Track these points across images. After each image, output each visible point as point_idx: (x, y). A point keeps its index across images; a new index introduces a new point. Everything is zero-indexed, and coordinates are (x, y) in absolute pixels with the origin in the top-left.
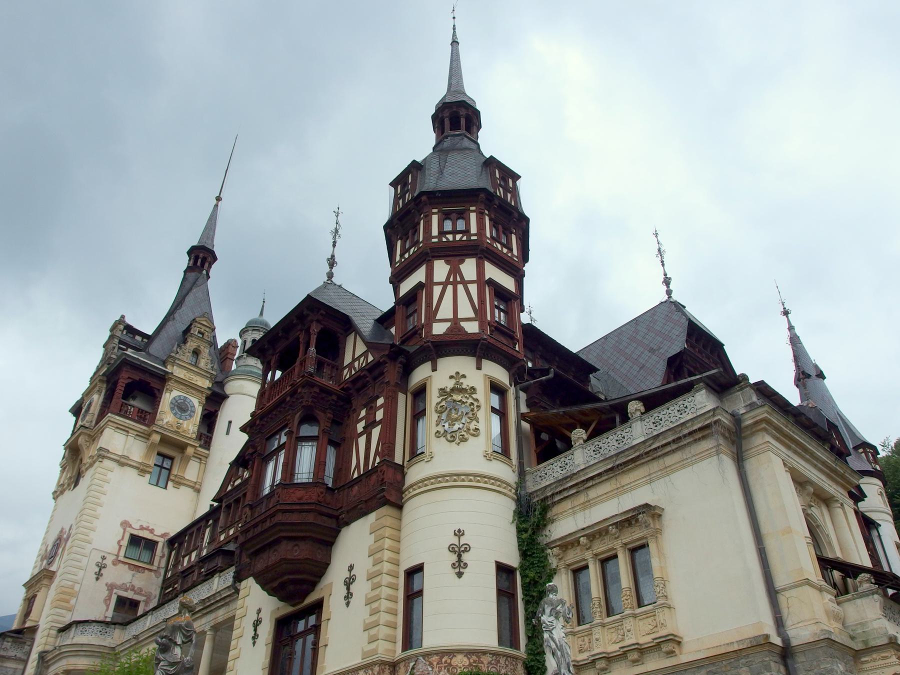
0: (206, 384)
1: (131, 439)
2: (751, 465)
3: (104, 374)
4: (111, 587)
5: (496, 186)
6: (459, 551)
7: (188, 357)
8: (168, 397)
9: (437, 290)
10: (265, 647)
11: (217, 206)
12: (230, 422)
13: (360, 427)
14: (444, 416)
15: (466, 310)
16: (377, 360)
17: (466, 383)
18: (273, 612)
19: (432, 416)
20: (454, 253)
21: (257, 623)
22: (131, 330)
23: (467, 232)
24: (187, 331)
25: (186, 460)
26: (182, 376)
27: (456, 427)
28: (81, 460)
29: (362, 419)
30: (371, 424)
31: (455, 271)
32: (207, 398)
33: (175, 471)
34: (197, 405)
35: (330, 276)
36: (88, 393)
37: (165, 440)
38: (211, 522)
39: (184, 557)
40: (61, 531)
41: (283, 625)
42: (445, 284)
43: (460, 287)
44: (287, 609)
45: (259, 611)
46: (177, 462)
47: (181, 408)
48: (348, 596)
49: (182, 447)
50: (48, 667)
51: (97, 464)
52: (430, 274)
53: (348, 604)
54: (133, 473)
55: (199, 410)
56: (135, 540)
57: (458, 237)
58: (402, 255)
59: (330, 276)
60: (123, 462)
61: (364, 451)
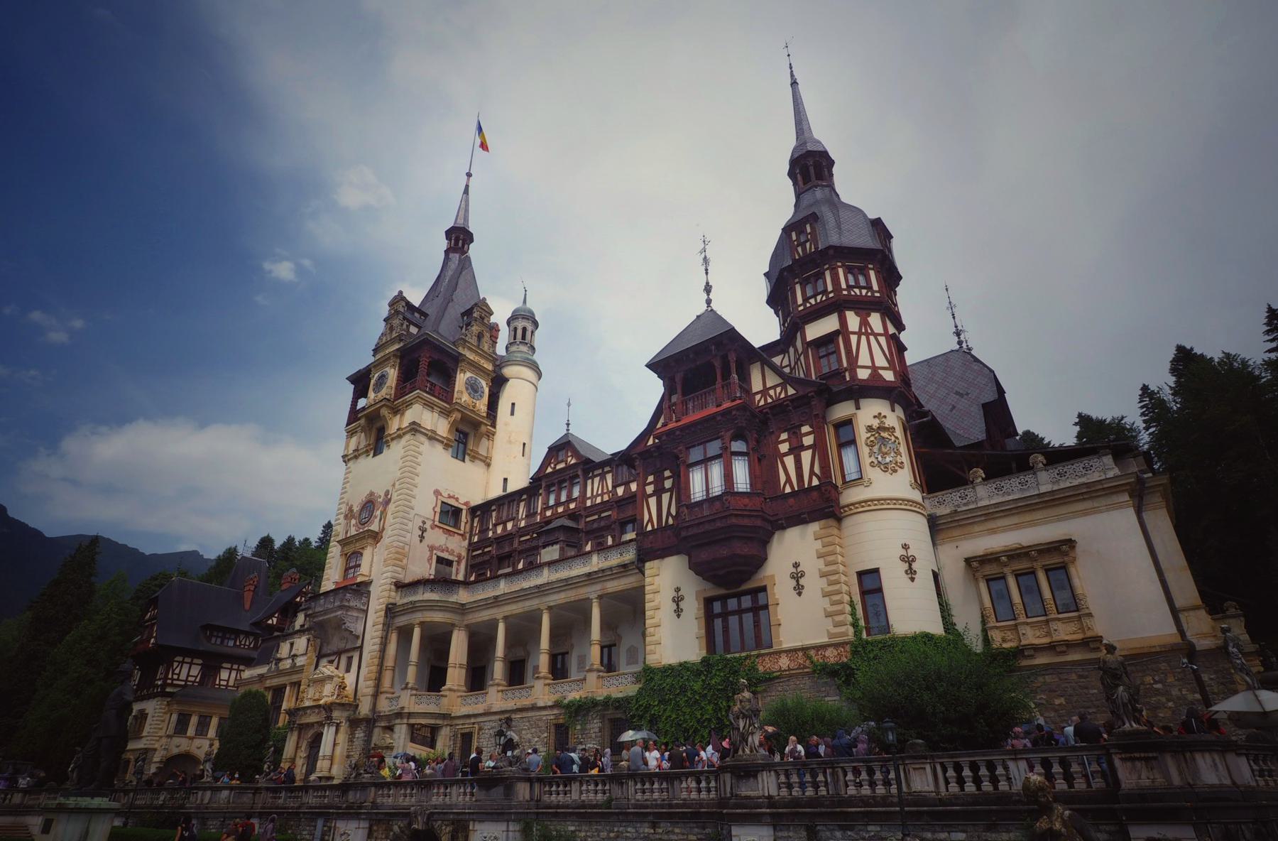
1: (436, 415)
2: (1145, 515)
4: (432, 548)
6: (909, 560)
7: (474, 341)
8: (462, 378)
9: (854, 339)
10: (695, 622)
11: (467, 186)
12: (513, 404)
13: (784, 448)
14: (876, 449)
15: (881, 361)
16: (801, 393)
18: (698, 593)
19: (865, 451)
20: (864, 307)
21: (678, 600)
22: (409, 306)
23: (869, 288)
24: (468, 313)
25: (479, 438)
27: (888, 459)
28: (382, 430)
29: (784, 441)
30: (796, 450)
31: (865, 323)
32: (492, 380)
33: (470, 446)
34: (485, 386)
35: (709, 302)
36: (378, 364)
37: (465, 419)
39: (495, 525)
40: (372, 494)
41: (708, 602)
42: (859, 334)
43: (872, 338)
44: (714, 591)
45: (678, 590)
47: (473, 388)
48: (799, 589)
49: (476, 425)
50: (393, 618)
51: (408, 437)
52: (843, 322)
53: (800, 594)
54: (439, 448)
55: (487, 390)
57: (864, 292)
58: (806, 300)
59: (709, 302)
60: (432, 437)
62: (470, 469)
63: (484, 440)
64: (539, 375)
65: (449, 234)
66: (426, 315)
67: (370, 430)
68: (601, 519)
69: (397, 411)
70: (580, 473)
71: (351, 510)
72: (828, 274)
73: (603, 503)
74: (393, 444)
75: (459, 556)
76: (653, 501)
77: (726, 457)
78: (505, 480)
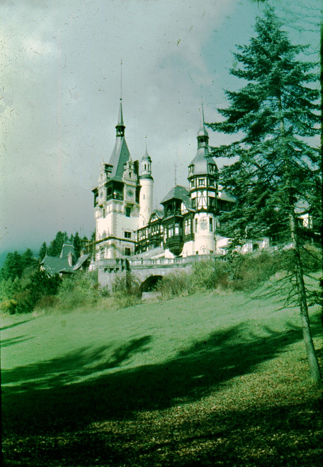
0: (134, 184)
3: (106, 184)
5: (210, 171)
9: (199, 199)
12: (144, 195)
13: (186, 224)
15: (204, 204)
17: (205, 219)
20: (202, 189)
23: (204, 185)
31: (202, 194)
34: (134, 190)
35: (176, 183)
37: (128, 204)
38: (147, 229)
40: (104, 231)
42: (200, 197)
46: (131, 209)
47: (130, 193)
49: (132, 205)
56: (126, 233)
59: (176, 183)
61: (187, 230)
64: (153, 182)
66: (112, 166)
67: (101, 210)
72: (195, 181)
74: (108, 215)
77: (174, 228)
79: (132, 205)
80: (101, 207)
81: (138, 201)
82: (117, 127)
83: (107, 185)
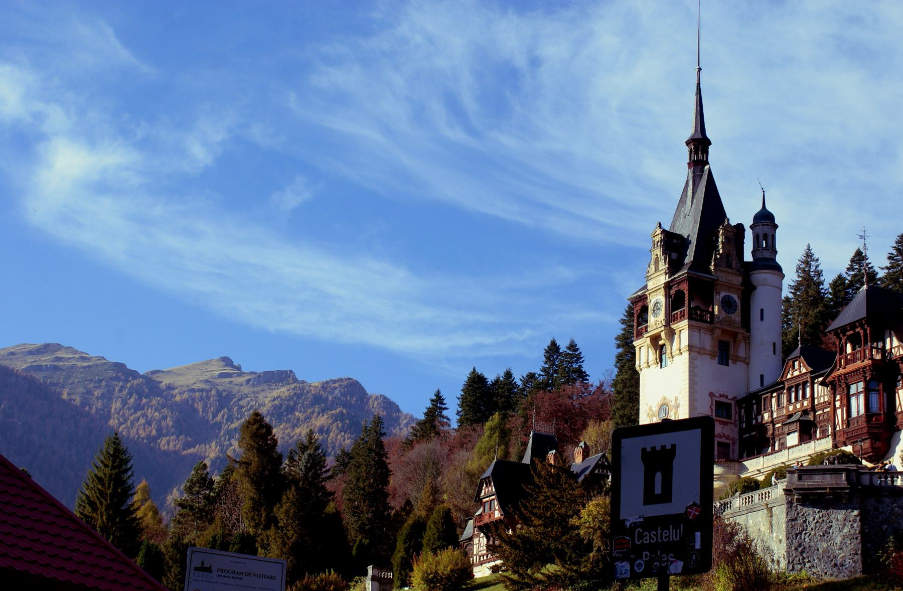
0: (737, 280)
1: (703, 335)
8: (718, 298)
11: (699, 84)
12: (762, 310)
26: (723, 280)
33: (731, 352)
38: (774, 395)
47: (727, 304)
49: (735, 335)
55: (739, 303)
62: (735, 370)
63: (743, 345)
65: (688, 143)
68: (824, 413)
69: (671, 334)
70: (809, 380)
71: (650, 409)
73: (825, 402)
75: (733, 439)
76: (839, 411)
78: (762, 376)
79: (735, 335)
80: (655, 339)
81: (746, 323)
82: (688, 143)
83: (668, 286)
